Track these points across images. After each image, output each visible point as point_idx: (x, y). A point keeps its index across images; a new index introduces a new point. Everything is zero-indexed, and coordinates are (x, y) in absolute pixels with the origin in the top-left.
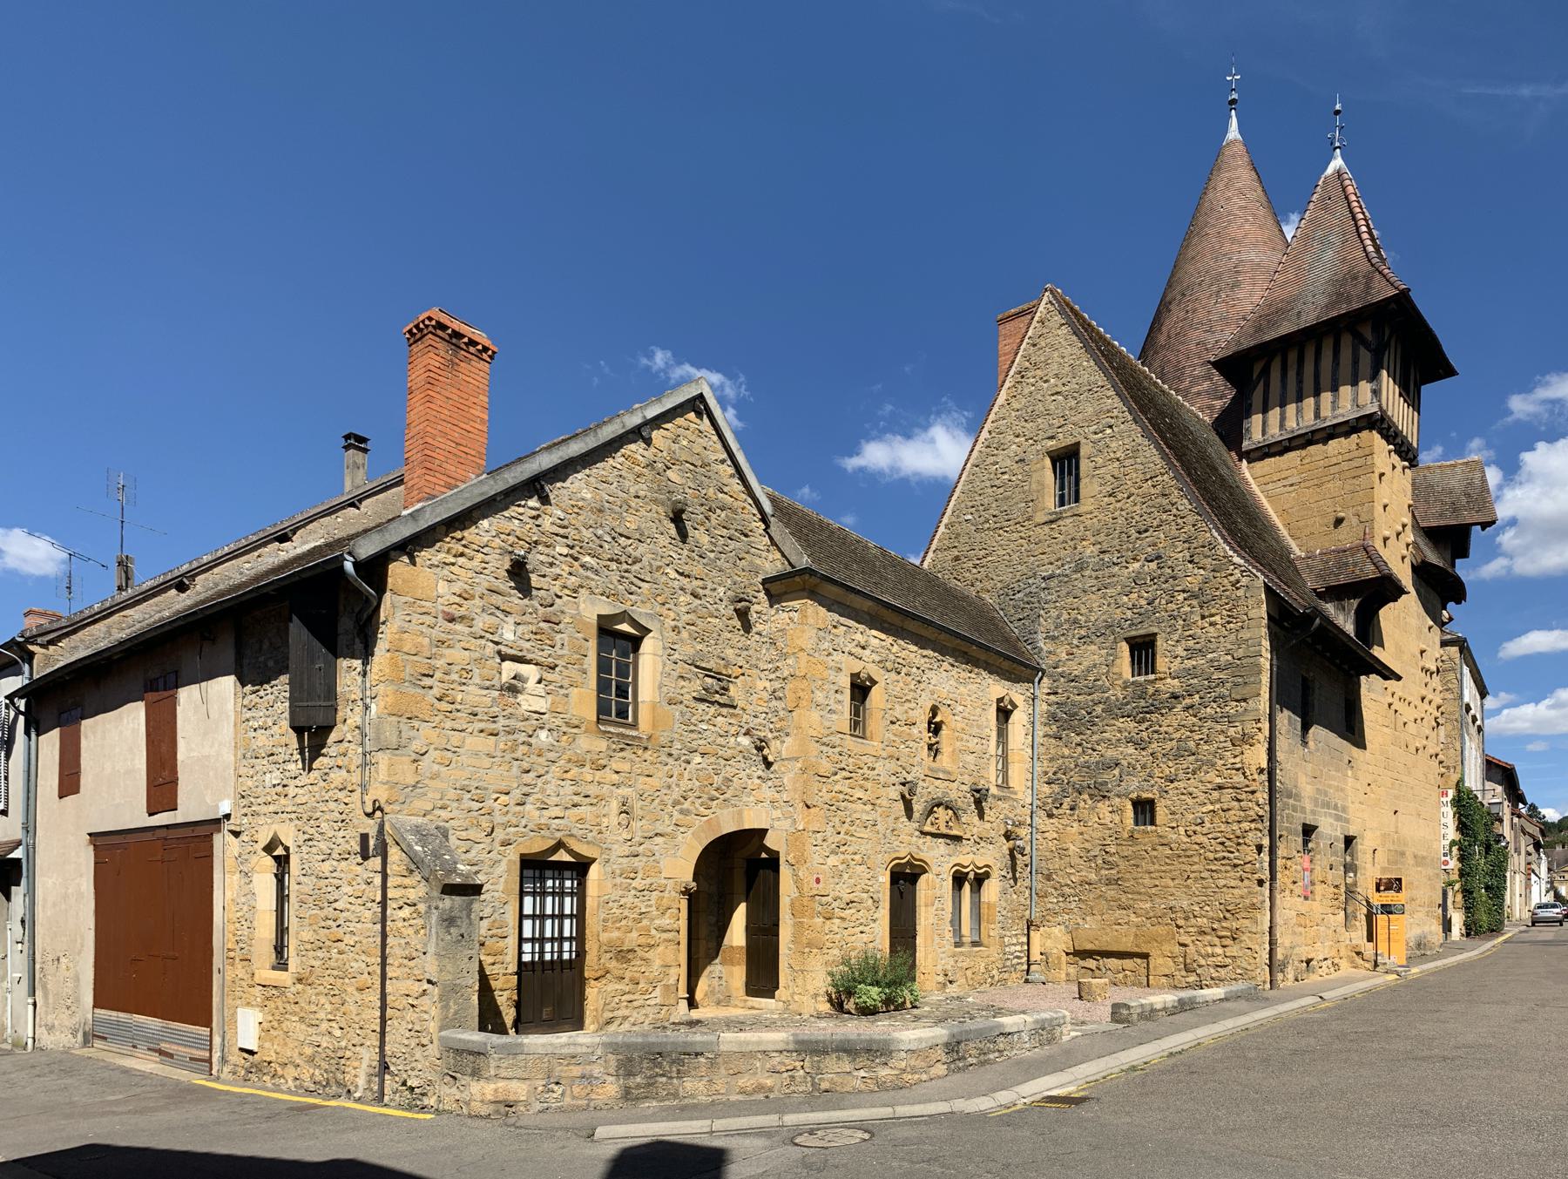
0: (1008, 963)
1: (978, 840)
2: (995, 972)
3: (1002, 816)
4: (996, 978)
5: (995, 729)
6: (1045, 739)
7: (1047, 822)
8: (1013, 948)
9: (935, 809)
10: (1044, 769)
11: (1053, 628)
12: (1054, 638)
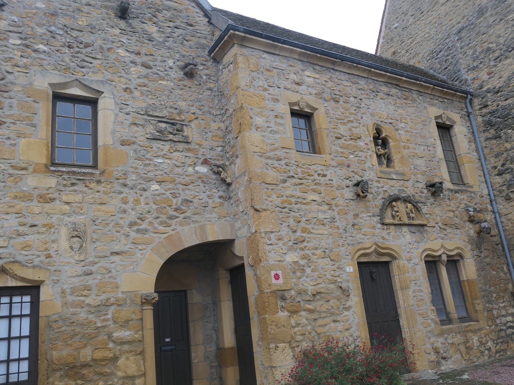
0: (503, 334)
1: (444, 227)
2: (490, 344)
3: (462, 206)
4: (493, 350)
5: (438, 138)
6: (487, 142)
7: (507, 206)
8: (504, 320)
9: (394, 203)
10: (492, 165)
11: (471, 62)
12: (474, 68)
